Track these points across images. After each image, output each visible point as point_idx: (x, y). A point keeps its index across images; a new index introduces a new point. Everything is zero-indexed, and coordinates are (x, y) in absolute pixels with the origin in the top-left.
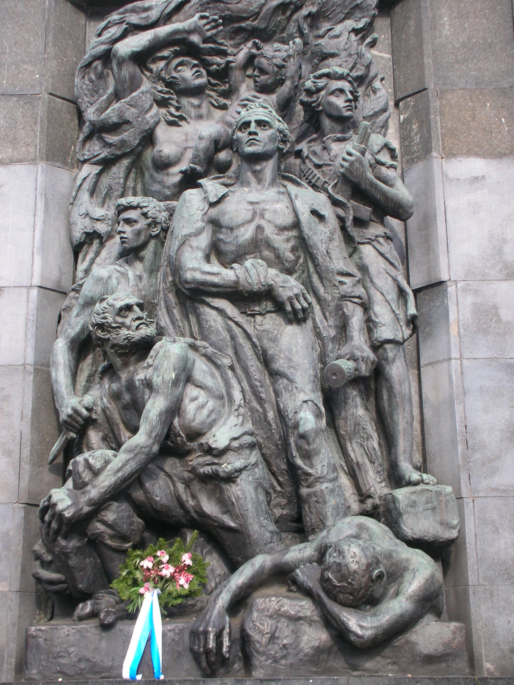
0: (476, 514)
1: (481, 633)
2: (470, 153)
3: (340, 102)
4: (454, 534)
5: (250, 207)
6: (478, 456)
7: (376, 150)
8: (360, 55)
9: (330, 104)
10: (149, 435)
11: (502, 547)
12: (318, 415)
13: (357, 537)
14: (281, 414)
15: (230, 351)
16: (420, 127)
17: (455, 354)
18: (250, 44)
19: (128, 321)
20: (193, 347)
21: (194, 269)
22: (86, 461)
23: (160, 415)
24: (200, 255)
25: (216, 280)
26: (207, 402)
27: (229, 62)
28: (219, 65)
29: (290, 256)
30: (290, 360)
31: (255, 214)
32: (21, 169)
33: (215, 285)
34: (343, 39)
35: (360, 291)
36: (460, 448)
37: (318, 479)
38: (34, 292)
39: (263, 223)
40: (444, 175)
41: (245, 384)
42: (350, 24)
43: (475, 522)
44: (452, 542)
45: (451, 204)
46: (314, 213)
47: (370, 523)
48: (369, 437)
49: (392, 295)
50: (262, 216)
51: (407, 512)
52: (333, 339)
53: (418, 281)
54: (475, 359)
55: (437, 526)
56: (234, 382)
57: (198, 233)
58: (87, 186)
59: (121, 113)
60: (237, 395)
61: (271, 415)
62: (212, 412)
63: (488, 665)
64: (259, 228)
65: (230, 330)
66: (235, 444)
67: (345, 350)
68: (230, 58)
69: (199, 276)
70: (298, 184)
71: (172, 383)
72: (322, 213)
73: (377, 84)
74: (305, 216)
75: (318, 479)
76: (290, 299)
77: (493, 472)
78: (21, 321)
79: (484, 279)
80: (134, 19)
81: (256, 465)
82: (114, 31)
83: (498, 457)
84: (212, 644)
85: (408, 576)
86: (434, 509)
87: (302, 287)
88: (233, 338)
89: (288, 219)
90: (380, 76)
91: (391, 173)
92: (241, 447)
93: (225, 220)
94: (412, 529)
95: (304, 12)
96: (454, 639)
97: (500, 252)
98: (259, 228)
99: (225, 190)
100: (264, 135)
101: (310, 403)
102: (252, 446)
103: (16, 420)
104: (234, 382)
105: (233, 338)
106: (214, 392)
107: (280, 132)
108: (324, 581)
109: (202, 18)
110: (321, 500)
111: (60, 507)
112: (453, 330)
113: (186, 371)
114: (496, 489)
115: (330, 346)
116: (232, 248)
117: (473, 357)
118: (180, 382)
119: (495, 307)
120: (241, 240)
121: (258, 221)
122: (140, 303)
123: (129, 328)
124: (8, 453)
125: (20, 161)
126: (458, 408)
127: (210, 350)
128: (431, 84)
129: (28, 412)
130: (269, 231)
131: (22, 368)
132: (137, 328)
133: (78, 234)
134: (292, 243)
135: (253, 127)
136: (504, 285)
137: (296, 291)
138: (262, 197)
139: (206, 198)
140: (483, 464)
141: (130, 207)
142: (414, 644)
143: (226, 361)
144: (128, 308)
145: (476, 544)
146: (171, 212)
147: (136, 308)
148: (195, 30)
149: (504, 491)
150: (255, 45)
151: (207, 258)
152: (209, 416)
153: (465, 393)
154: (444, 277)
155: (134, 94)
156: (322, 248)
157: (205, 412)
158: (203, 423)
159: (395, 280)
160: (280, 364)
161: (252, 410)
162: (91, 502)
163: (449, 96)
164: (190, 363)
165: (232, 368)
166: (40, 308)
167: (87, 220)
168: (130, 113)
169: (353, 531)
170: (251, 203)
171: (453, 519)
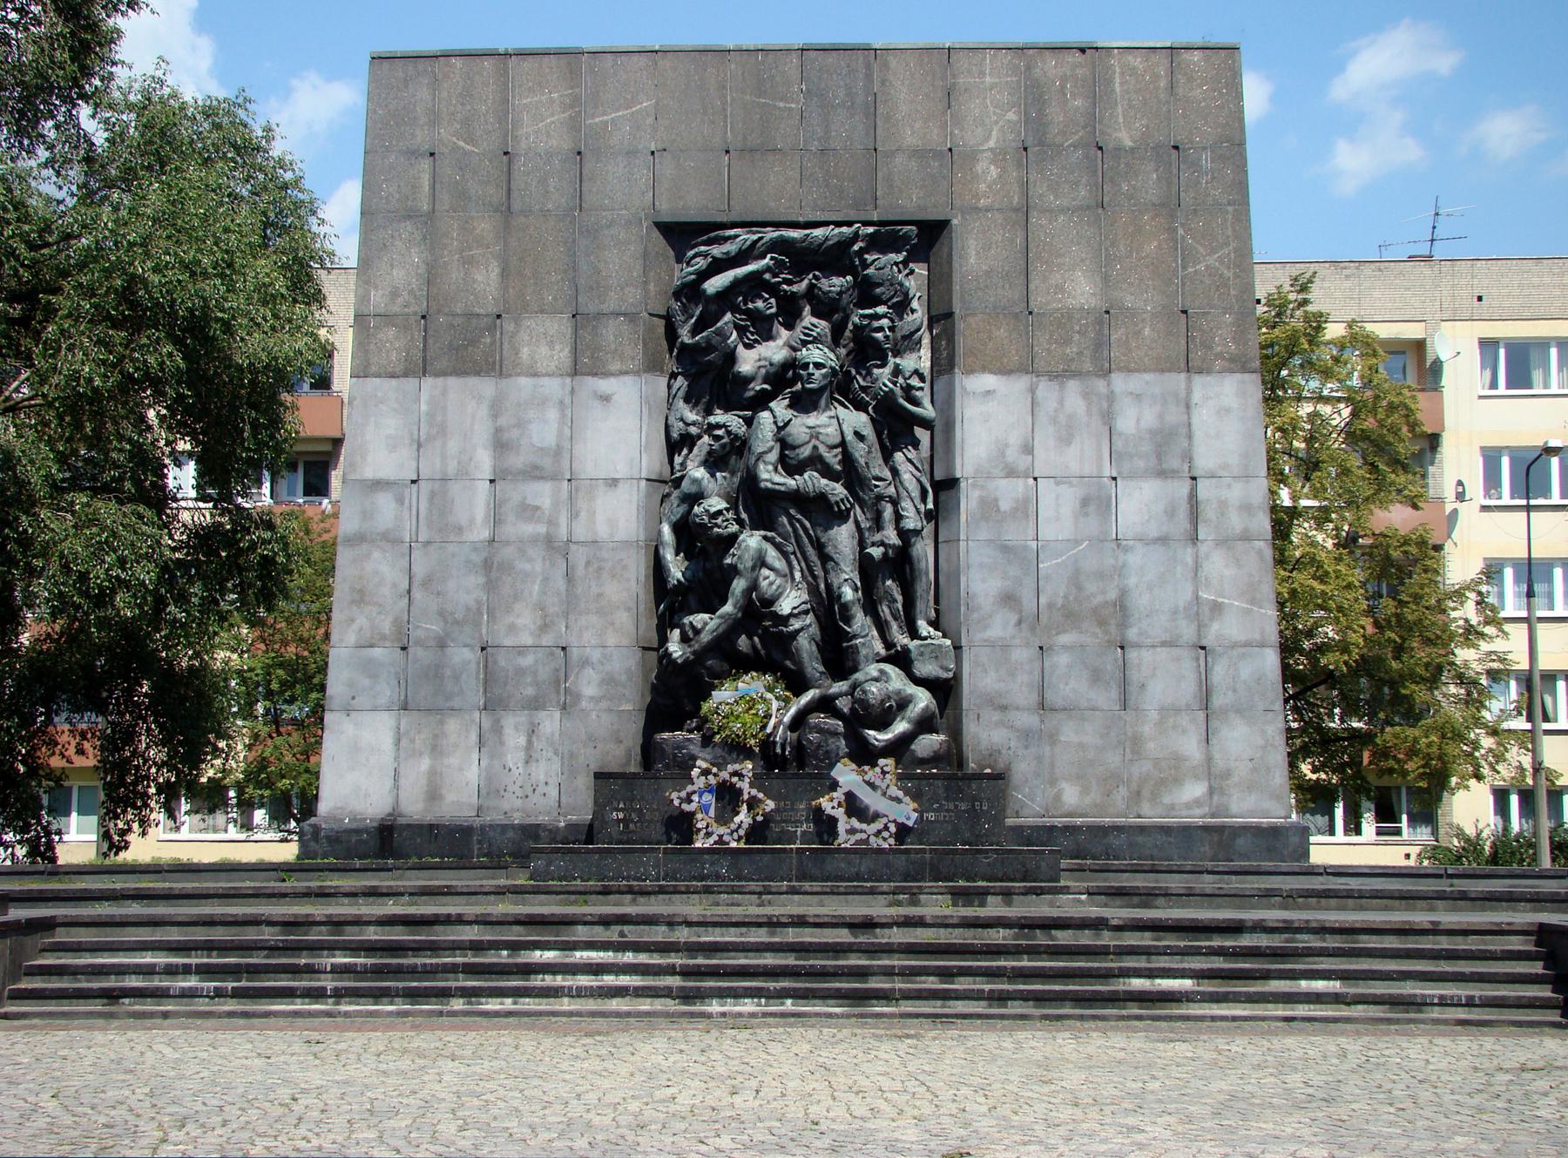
2: (984, 369)
3: (879, 335)
4: (951, 675)
5: (808, 431)
6: (975, 615)
7: (907, 375)
8: (901, 284)
9: (873, 338)
10: (735, 606)
12: (856, 589)
13: (876, 680)
14: (828, 586)
15: (793, 541)
16: (948, 344)
17: (962, 537)
18: (811, 276)
19: (719, 521)
20: (765, 538)
21: (766, 480)
22: (691, 623)
23: (743, 591)
24: (770, 468)
25: (783, 489)
27: (793, 293)
28: (785, 291)
29: (839, 468)
30: (836, 547)
31: (812, 437)
32: (629, 380)
33: (780, 492)
34: (887, 270)
35: (892, 490)
36: (962, 609)
37: (855, 636)
38: (643, 483)
39: (817, 443)
40: (964, 389)
41: (803, 564)
42: (893, 257)
44: (947, 680)
45: (967, 414)
46: (857, 434)
47: (888, 668)
48: (895, 601)
49: (916, 494)
50: (817, 438)
52: (870, 529)
53: (938, 476)
56: (795, 563)
57: (771, 450)
58: (681, 394)
59: (708, 340)
60: (798, 575)
61: (822, 586)
64: (815, 448)
65: (792, 525)
66: (796, 611)
67: (877, 537)
68: (795, 288)
69: (769, 485)
70: (846, 407)
72: (864, 433)
73: (915, 304)
74: (850, 437)
75: (855, 636)
76: (837, 503)
77: (986, 627)
78: (634, 507)
79: (989, 477)
80: (717, 251)
81: (810, 625)
82: (701, 263)
83: (990, 616)
84: (779, 750)
85: (911, 706)
87: (846, 492)
88: (795, 530)
89: (838, 440)
90: (918, 294)
91: (918, 394)
92: (800, 613)
93: (789, 440)
95: (856, 248)
97: (1003, 454)
98: (815, 448)
99: (789, 414)
100: (818, 374)
102: (806, 612)
103: (633, 584)
104: (795, 563)
105: (795, 530)
107: (831, 368)
108: (852, 709)
109: (772, 259)
110: (855, 649)
111: (675, 655)
112: (963, 518)
115: (867, 534)
116: (794, 462)
119: (996, 500)
120: (802, 457)
121: (814, 442)
123: (719, 527)
124: (629, 609)
125: (626, 373)
126: (963, 579)
127: (779, 539)
128: (957, 309)
129: (642, 578)
130: (822, 450)
133: (675, 435)
134: (840, 457)
135: (811, 369)
136: (1003, 483)
137: (842, 496)
138: (818, 423)
139: (775, 423)
141: (718, 426)
142: (914, 751)
143: (790, 549)
144: (720, 513)
146: (749, 422)
148: (768, 269)
150: (815, 277)
151: (776, 470)
154: (958, 475)
155: (719, 324)
156: (862, 461)
157: (774, 587)
159: (918, 480)
160: (829, 549)
161: (808, 583)
162: (694, 653)
163: (971, 320)
165: (794, 553)
166: (648, 495)
167: (681, 423)
168: (716, 340)
169: (875, 674)
170: (810, 428)
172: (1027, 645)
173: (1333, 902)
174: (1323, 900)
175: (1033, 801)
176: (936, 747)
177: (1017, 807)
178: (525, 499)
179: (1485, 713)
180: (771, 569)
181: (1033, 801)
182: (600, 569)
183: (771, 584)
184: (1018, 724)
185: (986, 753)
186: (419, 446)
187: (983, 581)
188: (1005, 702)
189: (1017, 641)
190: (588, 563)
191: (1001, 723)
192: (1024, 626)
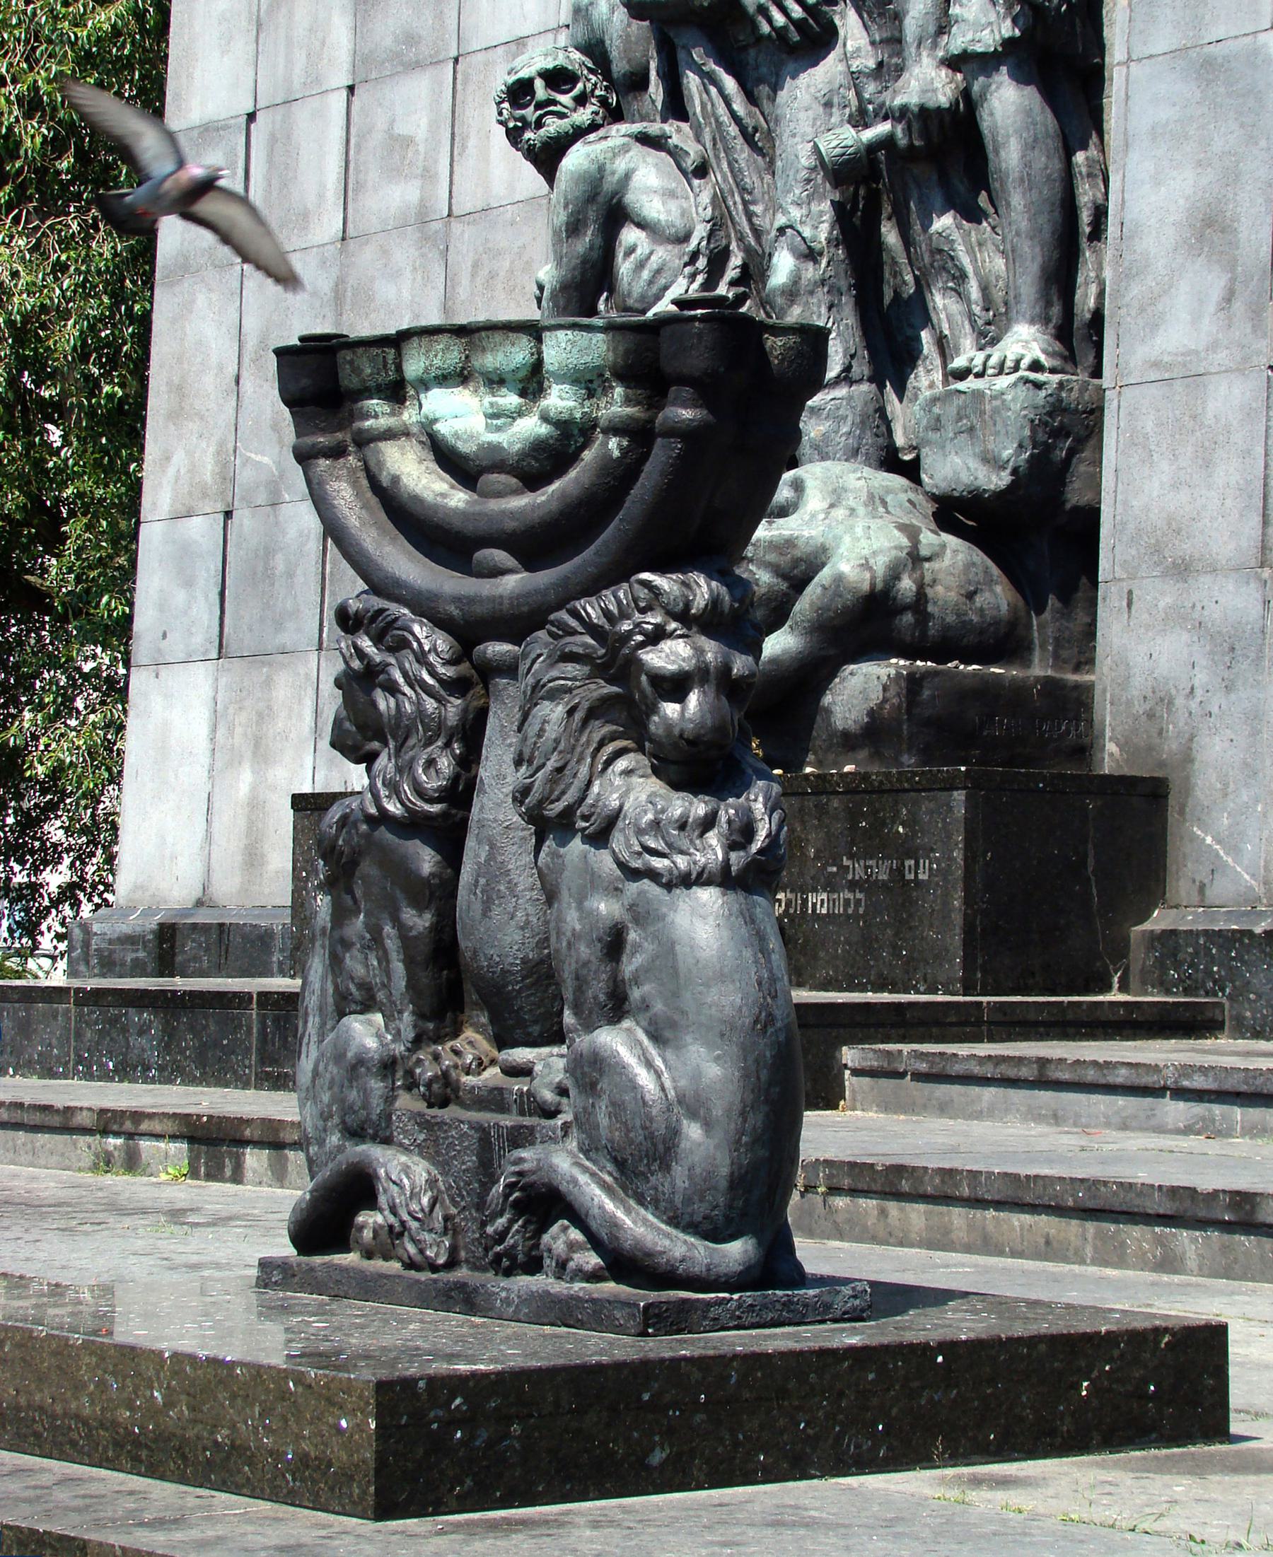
0: (1122, 424)
1: (1108, 682)
11: (1155, 494)
26: (651, 253)
43: (1118, 442)
51: (928, 443)
54: (1151, 56)
55: (974, 464)
62: (658, 271)
63: (1111, 747)
71: (567, 231)
77: (1154, 327)
86: (971, 429)
94: (931, 477)
96: (885, 700)
101: (789, 231)
106: (664, 231)
113: (601, 199)
114: (1156, 364)
117: (1147, 54)
118: (586, 226)
122: (547, 71)
131: (545, 201)
132: (539, 124)
140: (1142, 310)
145: (1115, 491)
147: (539, 84)
149: (1169, 367)
152: (651, 282)
153: (1127, 145)
157: (646, 274)
158: (643, 297)
164: (610, 183)
171: (1005, 448)
172: (1241, 368)
173: (917, 1214)
174: (893, 1207)
175: (1235, 850)
176: (876, 696)
177: (1202, 875)
178: (392, 122)
179: (55, 445)
180: (642, 225)
181: (1235, 850)
182: (492, 276)
183: (641, 265)
184: (1214, 614)
185: (1139, 708)
186: (259, 26)
187: (1157, 181)
188: (1186, 548)
189: (1222, 357)
190: (476, 265)
191: (1178, 617)
192: (1238, 306)
